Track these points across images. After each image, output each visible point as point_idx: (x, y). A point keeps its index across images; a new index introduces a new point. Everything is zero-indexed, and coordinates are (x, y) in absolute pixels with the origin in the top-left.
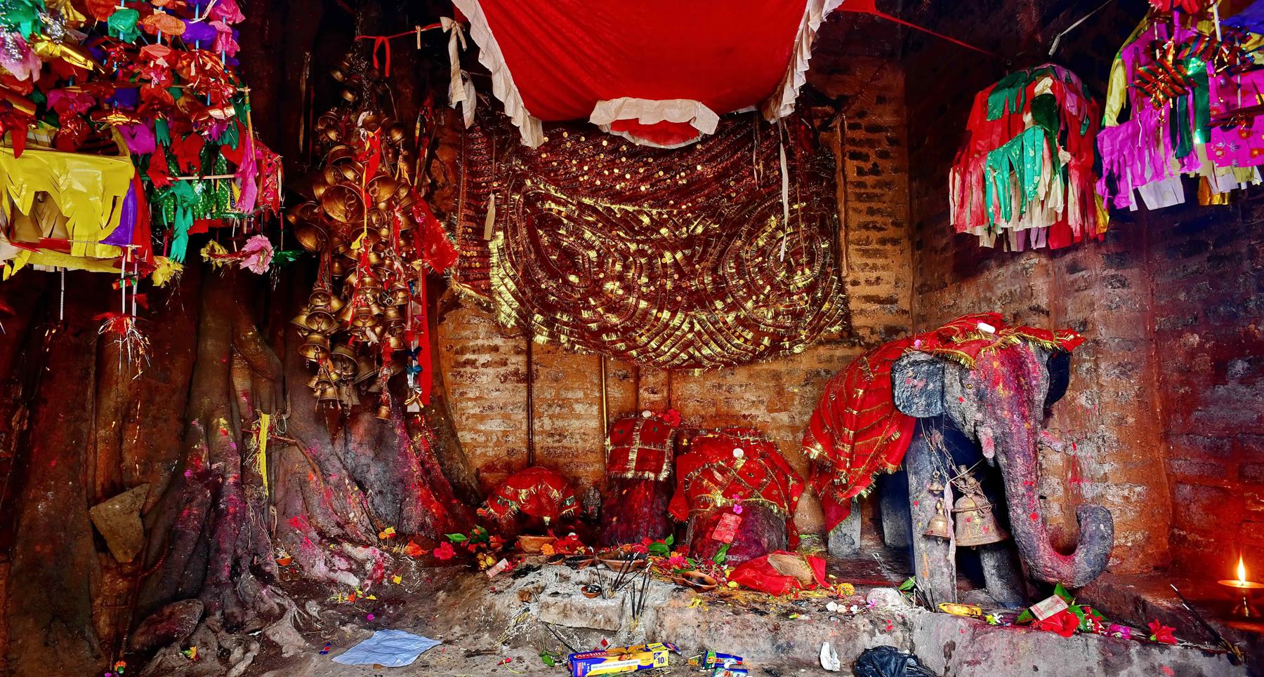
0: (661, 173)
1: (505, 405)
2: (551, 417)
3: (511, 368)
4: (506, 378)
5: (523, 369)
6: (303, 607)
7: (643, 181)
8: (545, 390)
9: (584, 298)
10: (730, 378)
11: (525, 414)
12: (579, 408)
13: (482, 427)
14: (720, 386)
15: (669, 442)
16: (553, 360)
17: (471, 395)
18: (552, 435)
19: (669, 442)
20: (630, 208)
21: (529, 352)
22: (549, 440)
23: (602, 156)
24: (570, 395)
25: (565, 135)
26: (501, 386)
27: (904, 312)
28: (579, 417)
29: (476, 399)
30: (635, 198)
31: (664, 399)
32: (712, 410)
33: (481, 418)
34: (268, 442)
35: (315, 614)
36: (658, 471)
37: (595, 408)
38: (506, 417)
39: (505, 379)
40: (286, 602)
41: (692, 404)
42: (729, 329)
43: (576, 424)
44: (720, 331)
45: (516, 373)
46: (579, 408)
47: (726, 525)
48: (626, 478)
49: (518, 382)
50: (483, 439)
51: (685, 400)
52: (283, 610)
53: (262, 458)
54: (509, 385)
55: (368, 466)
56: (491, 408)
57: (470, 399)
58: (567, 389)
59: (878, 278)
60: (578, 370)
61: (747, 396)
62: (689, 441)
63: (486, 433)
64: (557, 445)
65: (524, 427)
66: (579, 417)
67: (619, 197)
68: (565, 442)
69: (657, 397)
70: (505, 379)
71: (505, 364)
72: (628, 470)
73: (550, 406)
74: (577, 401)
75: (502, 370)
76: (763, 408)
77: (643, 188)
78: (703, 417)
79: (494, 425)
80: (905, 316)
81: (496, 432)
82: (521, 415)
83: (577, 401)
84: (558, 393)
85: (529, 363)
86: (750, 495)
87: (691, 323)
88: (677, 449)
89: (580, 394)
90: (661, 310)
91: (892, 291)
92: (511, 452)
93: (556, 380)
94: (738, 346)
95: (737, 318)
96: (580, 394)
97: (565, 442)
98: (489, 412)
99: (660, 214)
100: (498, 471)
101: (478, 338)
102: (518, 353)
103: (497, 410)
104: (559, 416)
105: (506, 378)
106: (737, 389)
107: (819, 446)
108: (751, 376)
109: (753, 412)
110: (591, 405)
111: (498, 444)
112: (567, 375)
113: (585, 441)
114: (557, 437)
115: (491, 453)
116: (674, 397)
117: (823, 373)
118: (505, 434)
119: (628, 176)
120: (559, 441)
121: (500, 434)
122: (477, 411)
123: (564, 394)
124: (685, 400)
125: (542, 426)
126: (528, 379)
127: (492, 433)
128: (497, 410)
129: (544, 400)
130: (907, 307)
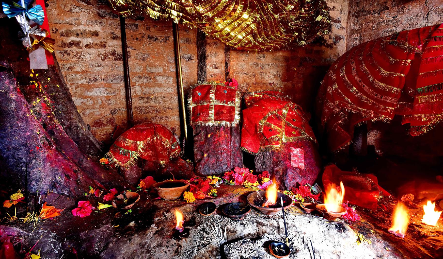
2: (141, 86)
3: (109, 50)
4: (105, 57)
5: (119, 51)
10: (262, 59)
11: (122, 84)
13: (90, 94)
14: (257, 65)
16: (140, 45)
17: (78, 69)
18: (142, 98)
22: (141, 102)
24: (154, 70)
26: (102, 63)
27: (344, 28)
28: (160, 85)
29: (83, 72)
33: (88, 87)
38: (108, 86)
41: (242, 75)
43: (158, 90)
45: (113, 53)
46: (160, 79)
49: (115, 60)
50: (91, 102)
54: (108, 62)
56: (95, 79)
57: (77, 73)
58: (151, 66)
59: (334, 7)
60: (158, 53)
63: (92, 98)
64: (146, 105)
66: (160, 85)
68: (152, 103)
71: (104, 46)
73: (140, 78)
74: (159, 74)
75: (102, 51)
76: (279, 79)
78: (248, 84)
80: (344, 31)
83: (159, 74)
84: (145, 69)
85: (124, 47)
89: (161, 70)
91: (339, 16)
92: (113, 111)
93: (143, 60)
97: (152, 103)
98: (94, 83)
100: (105, 125)
101: (80, 24)
102: (114, 38)
104: (147, 85)
105: (105, 57)
110: (168, 77)
112: (151, 57)
114: (146, 100)
115: (97, 112)
116: (231, 71)
117: (308, 60)
118: (108, 98)
120: (147, 102)
121: (104, 99)
122: (84, 81)
123: (149, 69)
125: (135, 92)
127: (97, 98)
129: (136, 74)
130: (345, 26)
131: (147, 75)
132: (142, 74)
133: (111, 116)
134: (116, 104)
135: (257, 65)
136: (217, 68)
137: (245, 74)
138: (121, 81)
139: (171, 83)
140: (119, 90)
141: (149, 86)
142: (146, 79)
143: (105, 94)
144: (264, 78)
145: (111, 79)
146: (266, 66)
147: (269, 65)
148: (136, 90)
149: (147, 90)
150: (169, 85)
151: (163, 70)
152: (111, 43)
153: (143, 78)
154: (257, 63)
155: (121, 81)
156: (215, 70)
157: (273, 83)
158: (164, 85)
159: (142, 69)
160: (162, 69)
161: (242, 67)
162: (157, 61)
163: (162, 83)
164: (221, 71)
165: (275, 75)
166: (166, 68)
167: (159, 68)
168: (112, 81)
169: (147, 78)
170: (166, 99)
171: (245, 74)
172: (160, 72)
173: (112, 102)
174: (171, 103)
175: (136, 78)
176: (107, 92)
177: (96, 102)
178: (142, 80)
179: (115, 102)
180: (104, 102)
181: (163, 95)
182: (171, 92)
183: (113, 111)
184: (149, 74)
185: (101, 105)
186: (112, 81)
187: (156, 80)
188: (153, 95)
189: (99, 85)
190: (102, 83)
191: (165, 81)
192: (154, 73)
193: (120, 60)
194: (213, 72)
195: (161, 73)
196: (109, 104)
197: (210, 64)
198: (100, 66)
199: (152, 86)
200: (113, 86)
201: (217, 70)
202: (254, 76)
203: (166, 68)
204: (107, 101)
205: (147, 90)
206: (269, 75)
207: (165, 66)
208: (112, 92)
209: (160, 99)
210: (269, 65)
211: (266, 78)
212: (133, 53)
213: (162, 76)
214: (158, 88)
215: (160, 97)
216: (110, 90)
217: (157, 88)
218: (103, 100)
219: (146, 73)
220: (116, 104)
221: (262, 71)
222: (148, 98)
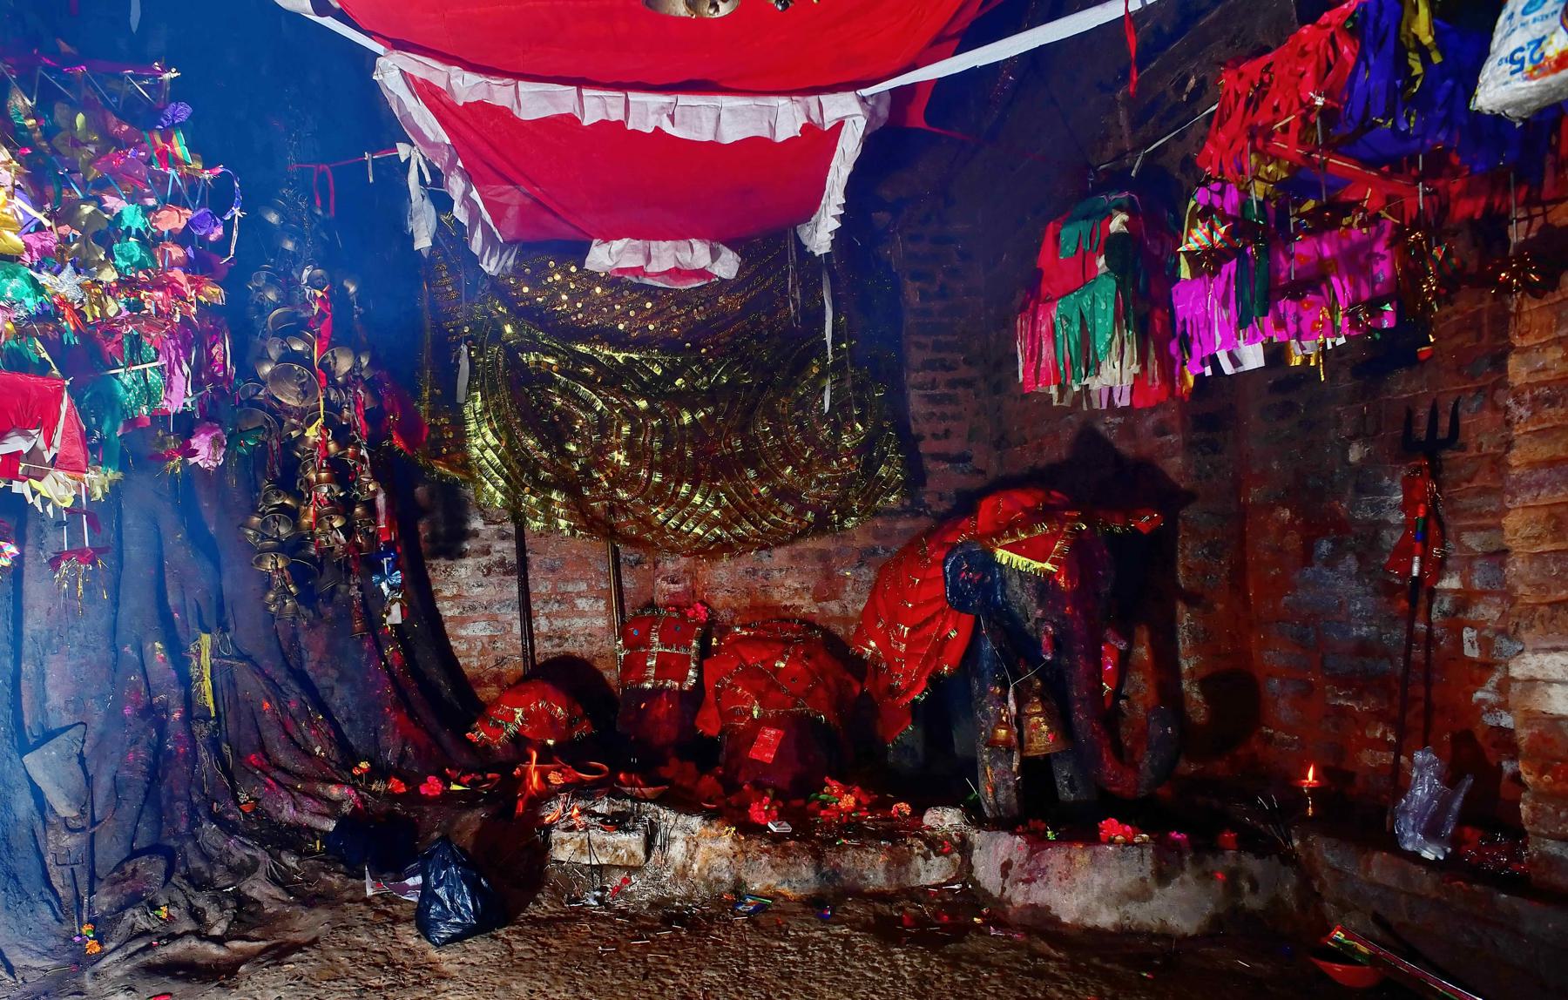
0: (674, 308)
3: (496, 557)
4: (489, 571)
5: (512, 558)
6: (279, 858)
7: (651, 318)
8: (541, 586)
9: (585, 470)
10: (766, 561)
12: (582, 604)
13: (463, 633)
14: (755, 572)
15: (694, 644)
17: (447, 593)
18: (550, 638)
19: (694, 644)
20: (635, 356)
21: (520, 537)
23: (598, 290)
24: (570, 588)
25: (552, 264)
26: (484, 581)
28: (582, 614)
29: (454, 597)
30: (643, 343)
32: (747, 602)
33: (462, 621)
34: (212, 667)
35: (294, 864)
36: (683, 678)
37: (602, 603)
38: (493, 619)
39: (489, 571)
40: (260, 854)
42: (763, 503)
43: (579, 623)
44: (753, 505)
45: (502, 563)
46: (582, 604)
47: (766, 741)
48: (644, 689)
49: (505, 574)
50: (465, 646)
51: (713, 590)
52: (255, 863)
53: (207, 685)
54: (494, 579)
55: (332, 689)
56: (473, 608)
57: (446, 599)
58: (566, 580)
61: (788, 582)
62: (719, 640)
63: (468, 640)
65: (517, 629)
66: (582, 614)
67: (619, 341)
70: (489, 571)
72: (647, 679)
73: (546, 602)
74: (579, 595)
75: (484, 560)
77: (651, 327)
79: (478, 630)
82: (512, 616)
85: (521, 550)
86: (795, 705)
87: (718, 499)
88: (705, 651)
90: (679, 484)
92: (500, 661)
93: (553, 570)
94: (773, 523)
95: (772, 489)
96: (583, 587)
98: (470, 614)
99: (673, 362)
100: (486, 685)
102: (503, 538)
104: (558, 615)
105: (489, 571)
106: (776, 574)
107: (873, 644)
108: (792, 558)
109: (797, 602)
110: (597, 599)
111: (483, 652)
113: (591, 644)
118: (492, 639)
119: (632, 313)
121: (485, 640)
122: (456, 612)
123: (562, 587)
124: (713, 590)
126: (522, 568)
127: (476, 638)
135: (755, 572)
139: (602, 608)
140: (511, 625)
148: (542, 624)
149: (558, 623)
150: (598, 614)
152: (499, 546)
175: (540, 603)
183: (500, 661)
205: (558, 623)
212: (534, 560)
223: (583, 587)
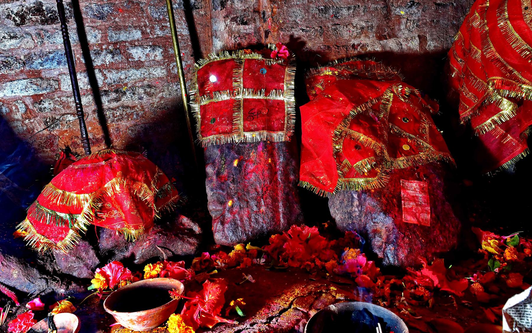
1: (29, 58)
11: (64, 68)
12: (137, 53)
24: (123, 36)
28: (139, 65)
31: (257, 31)
38: (35, 75)
43: (135, 74)
58: (118, 28)
66: (139, 65)
69: (249, 28)
74: (133, 44)
81: (22, 99)
83: (133, 44)
84: (105, 36)
93: (102, 18)
103: (17, 67)
110: (154, 47)
118: (37, 99)
121: (28, 101)
123: (114, 37)
127: (16, 100)
128: (17, 67)
131: (111, 47)
132: (100, 45)
133: (48, 133)
134: (55, 109)
136: (246, 24)
137: (303, 30)
138: (59, 63)
139: (159, 58)
140: (58, 81)
141: (117, 69)
142: (110, 56)
143: (31, 92)
144: (342, 36)
145: (40, 61)
146: (345, 12)
147: (349, 9)
151: (143, 33)
153: (104, 52)
154: (325, 7)
155: (59, 63)
156: (242, 27)
157: (359, 45)
158: (146, 63)
159: (99, 36)
160: (139, 33)
161: (296, 17)
162: (129, 17)
163: (143, 60)
164: (255, 27)
165: (362, 28)
166: (148, 31)
167: (134, 31)
168: (41, 64)
169: (111, 52)
170: (153, 91)
171: (303, 30)
172: (136, 37)
173: (46, 105)
174: (162, 98)
176: (34, 87)
177: (14, 108)
178: (102, 57)
179: (52, 105)
180: (31, 107)
181: (146, 82)
182: (161, 75)
184: (115, 44)
185: (26, 112)
186: (41, 64)
187: (129, 56)
188: (126, 85)
189: (17, 75)
190: (22, 71)
191: (147, 55)
192: (125, 42)
193: (52, 23)
194: (239, 32)
195: (138, 40)
196: (40, 109)
197: (232, 16)
198: (15, 37)
199: (123, 68)
200: (43, 74)
201: (247, 27)
202: (322, 33)
203: (148, 31)
204: (37, 105)
206: (352, 29)
207: (145, 26)
208: (44, 86)
209: (141, 91)
210: (349, 9)
211: (346, 35)
213: (141, 46)
214: (135, 71)
215: (142, 87)
216: (39, 83)
217: (133, 71)
218: (27, 103)
219: (109, 44)
220: (55, 109)
221: (337, 21)
222: (117, 91)
223: (137, 35)
